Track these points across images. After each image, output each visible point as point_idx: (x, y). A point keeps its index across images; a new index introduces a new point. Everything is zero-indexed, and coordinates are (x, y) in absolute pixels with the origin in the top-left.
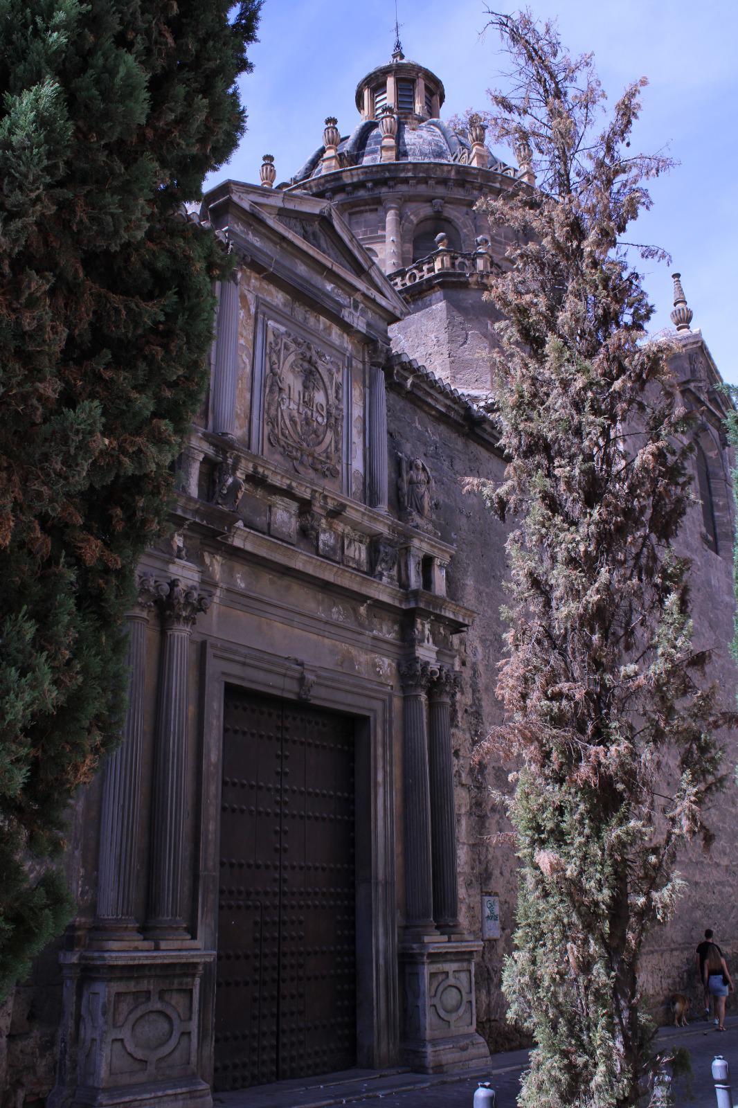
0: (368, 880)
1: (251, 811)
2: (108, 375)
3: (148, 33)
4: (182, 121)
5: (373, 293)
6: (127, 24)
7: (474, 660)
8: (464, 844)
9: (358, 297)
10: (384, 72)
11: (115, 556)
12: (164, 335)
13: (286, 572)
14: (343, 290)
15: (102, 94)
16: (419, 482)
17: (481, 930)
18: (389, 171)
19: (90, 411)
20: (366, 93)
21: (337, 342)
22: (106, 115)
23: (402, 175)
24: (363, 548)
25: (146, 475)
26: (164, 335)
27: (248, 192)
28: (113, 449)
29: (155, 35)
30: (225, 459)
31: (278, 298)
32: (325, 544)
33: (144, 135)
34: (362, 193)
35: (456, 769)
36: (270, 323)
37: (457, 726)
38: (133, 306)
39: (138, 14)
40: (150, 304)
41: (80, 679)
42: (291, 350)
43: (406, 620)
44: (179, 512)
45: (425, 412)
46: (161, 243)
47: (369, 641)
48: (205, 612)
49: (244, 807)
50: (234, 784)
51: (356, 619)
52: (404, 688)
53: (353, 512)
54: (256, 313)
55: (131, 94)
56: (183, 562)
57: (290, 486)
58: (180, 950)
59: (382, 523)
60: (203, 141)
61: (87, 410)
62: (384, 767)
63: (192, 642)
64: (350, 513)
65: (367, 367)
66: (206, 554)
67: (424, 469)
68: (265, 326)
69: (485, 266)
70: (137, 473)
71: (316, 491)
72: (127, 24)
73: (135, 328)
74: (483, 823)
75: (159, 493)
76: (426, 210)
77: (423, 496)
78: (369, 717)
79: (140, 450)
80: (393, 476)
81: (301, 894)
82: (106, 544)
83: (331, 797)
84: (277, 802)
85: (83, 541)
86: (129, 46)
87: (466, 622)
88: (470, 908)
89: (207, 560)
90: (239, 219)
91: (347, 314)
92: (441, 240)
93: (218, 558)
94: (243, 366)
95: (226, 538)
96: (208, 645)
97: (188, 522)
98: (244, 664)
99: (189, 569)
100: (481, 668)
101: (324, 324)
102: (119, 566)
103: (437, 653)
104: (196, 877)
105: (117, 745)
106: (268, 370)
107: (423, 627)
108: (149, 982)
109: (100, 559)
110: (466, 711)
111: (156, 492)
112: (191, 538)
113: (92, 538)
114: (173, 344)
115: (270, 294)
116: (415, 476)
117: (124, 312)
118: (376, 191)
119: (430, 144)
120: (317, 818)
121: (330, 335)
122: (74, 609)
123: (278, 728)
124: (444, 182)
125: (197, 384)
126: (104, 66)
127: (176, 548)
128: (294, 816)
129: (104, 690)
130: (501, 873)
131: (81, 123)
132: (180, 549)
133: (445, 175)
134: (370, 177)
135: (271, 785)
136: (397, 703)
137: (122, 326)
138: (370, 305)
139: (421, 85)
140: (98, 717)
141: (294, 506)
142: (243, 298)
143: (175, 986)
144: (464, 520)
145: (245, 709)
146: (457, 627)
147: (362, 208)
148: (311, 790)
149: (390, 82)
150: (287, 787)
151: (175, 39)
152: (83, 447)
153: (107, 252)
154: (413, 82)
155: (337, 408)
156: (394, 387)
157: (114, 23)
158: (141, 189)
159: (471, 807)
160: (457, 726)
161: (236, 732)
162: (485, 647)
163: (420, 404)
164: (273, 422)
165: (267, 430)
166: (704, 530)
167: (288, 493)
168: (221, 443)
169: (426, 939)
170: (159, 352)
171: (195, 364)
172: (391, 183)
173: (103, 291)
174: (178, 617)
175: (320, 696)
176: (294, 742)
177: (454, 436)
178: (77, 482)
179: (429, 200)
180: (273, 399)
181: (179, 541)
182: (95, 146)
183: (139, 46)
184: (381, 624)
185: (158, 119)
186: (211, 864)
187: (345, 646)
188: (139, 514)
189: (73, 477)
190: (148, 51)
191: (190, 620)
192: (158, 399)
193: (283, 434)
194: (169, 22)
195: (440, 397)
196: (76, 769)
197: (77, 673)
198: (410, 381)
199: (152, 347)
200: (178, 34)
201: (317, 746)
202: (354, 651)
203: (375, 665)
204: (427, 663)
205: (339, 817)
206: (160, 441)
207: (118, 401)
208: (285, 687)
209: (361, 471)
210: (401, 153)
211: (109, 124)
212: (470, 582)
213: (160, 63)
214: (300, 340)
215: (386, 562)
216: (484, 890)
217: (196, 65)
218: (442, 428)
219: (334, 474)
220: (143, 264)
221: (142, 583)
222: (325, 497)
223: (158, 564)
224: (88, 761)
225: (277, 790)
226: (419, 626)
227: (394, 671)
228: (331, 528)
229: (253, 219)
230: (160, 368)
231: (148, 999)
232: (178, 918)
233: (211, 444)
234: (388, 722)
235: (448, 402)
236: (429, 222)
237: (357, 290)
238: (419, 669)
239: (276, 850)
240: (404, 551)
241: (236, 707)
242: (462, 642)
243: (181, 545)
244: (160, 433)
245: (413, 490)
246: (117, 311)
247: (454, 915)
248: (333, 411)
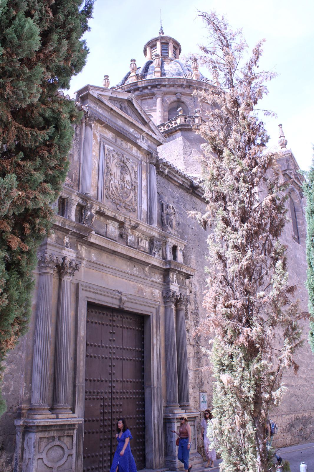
0: (150, 386)
1: (99, 357)
2: (22, 163)
3: (41, 11)
4: (56, 51)
5: (150, 133)
6: (31, 7)
7: (195, 290)
8: (192, 370)
9: (144, 135)
10: (156, 40)
11: (26, 245)
12: (48, 145)
13: (114, 253)
14: (137, 131)
15: (17, 36)
16: (171, 214)
17: (199, 407)
18: (158, 81)
19: (11, 179)
20: (148, 49)
21: (135, 154)
22: (20, 46)
23: (163, 83)
24: (147, 242)
25: (40, 209)
26: (48, 145)
27: (96, 90)
28: (23, 197)
29: (44, 12)
30: (87, 204)
31: (110, 135)
32: (130, 241)
33: (39, 57)
34: (146, 91)
35: (188, 337)
36: (106, 146)
38: (34, 133)
39: (36, 3)
40: (42, 132)
41: (7, 302)
42: (115, 157)
43: (166, 273)
44: (67, 227)
45: (173, 184)
46: (48, 105)
47: (150, 282)
48: (78, 271)
49: (96, 355)
50: (91, 345)
51: (144, 273)
52: (165, 303)
53: (142, 227)
54: (100, 141)
55: (31, 37)
56: (69, 249)
57: (115, 216)
58: (67, 418)
59: (155, 231)
60: (66, 59)
61: (9, 178)
62: (156, 337)
63: (73, 283)
64: (141, 227)
66: (79, 245)
67: (173, 208)
68: (104, 147)
69: (199, 122)
70: (34, 207)
71: (126, 218)
72: (31, 7)
73: (35, 143)
74: (200, 361)
75: (46, 217)
76: (174, 98)
77: (172, 220)
78: (149, 316)
79: (36, 197)
80: (160, 211)
81: (121, 393)
82: (23, 240)
83: (134, 350)
84: (110, 353)
85: (11, 238)
86: (32, 17)
87: (192, 274)
88: (195, 398)
89: (79, 248)
90: (92, 101)
91: (139, 142)
92: (180, 111)
93: (84, 247)
94: (94, 164)
95: (87, 238)
96: (80, 285)
97: (70, 232)
98: (95, 293)
99: (71, 252)
100: (198, 294)
101: (130, 146)
102: (28, 250)
103: (179, 287)
104: (75, 386)
105: (27, 331)
106: (105, 166)
107: (173, 276)
109: (19, 247)
110: (192, 312)
111: (45, 217)
112: (72, 238)
113: (15, 237)
114: (53, 150)
115: (107, 134)
116: (169, 211)
117: (30, 136)
118: (153, 90)
119: (175, 70)
120: (127, 360)
121: (132, 151)
122: (5, 269)
123: (110, 320)
124: (181, 86)
125: (64, 168)
126: (19, 24)
127: (65, 243)
128: (117, 359)
129: (20, 306)
130: (208, 383)
131: (8, 50)
132: (67, 244)
133: (182, 83)
134: (150, 84)
135: (107, 346)
136: (162, 309)
137: (29, 142)
138: (149, 138)
139: (171, 45)
140: (17, 318)
141: (117, 224)
142: (95, 135)
143: (66, 434)
144: (190, 230)
145: (96, 313)
146: (188, 276)
147: (146, 97)
148: (125, 347)
149: (158, 44)
150: (114, 346)
151: (54, 15)
152: (7, 195)
153: (21, 109)
154: (168, 44)
155: (135, 182)
156: (160, 173)
157: (25, 6)
158: (36, 80)
159: (194, 354)
160: (188, 319)
161: (92, 322)
162: (200, 285)
163: (171, 180)
164: (108, 188)
165: (105, 192)
166: (293, 233)
167: (114, 219)
168: (85, 197)
169: (176, 412)
170: (46, 154)
171: (63, 159)
172: (159, 87)
173: (20, 126)
174: (67, 273)
175: (128, 307)
176: (118, 326)
177: (186, 194)
178: (5, 211)
179: (175, 94)
180: (107, 179)
181: (67, 240)
182: (15, 60)
183: (37, 17)
184: (155, 275)
185: (45, 49)
186: (81, 380)
187: (139, 285)
188: (37, 226)
189: (3, 208)
190: (41, 19)
191: (72, 274)
192: (46, 175)
193: (112, 194)
194: (51, 7)
195: (180, 177)
196: (7, 342)
197: (6, 299)
198: (166, 171)
199: (43, 151)
200: (55, 13)
201: (127, 328)
202: (143, 287)
203: (152, 293)
204: (175, 292)
205: (137, 359)
206: (45, 193)
207: (26, 175)
208: (114, 303)
209: (146, 209)
210: (163, 74)
211: (21, 50)
212: (193, 256)
213: (46, 25)
214: (119, 153)
215: (157, 248)
216: (201, 390)
217: (63, 26)
218: (181, 190)
219: (134, 210)
220: (39, 114)
221: (51, 258)
222: (130, 220)
223: (58, 250)
224: (12, 339)
225: (110, 348)
226: (171, 276)
227: (161, 295)
228: (133, 234)
229: (99, 101)
230: (47, 161)
231: (54, 440)
232: (67, 404)
233: (81, 198)
234: (158, 318)
235: (183, 180)
236: (175, 103)
237: (144, 131)
238: (171, 294)
239: (110, 374)
240: (165, 243)
241: (92, 312)
242: (190, 283)
243: (68, 241)
244: (45, 189)
245: (168, 217)
246: (27, 135)
247: (188, 401)
248: (134, 184)
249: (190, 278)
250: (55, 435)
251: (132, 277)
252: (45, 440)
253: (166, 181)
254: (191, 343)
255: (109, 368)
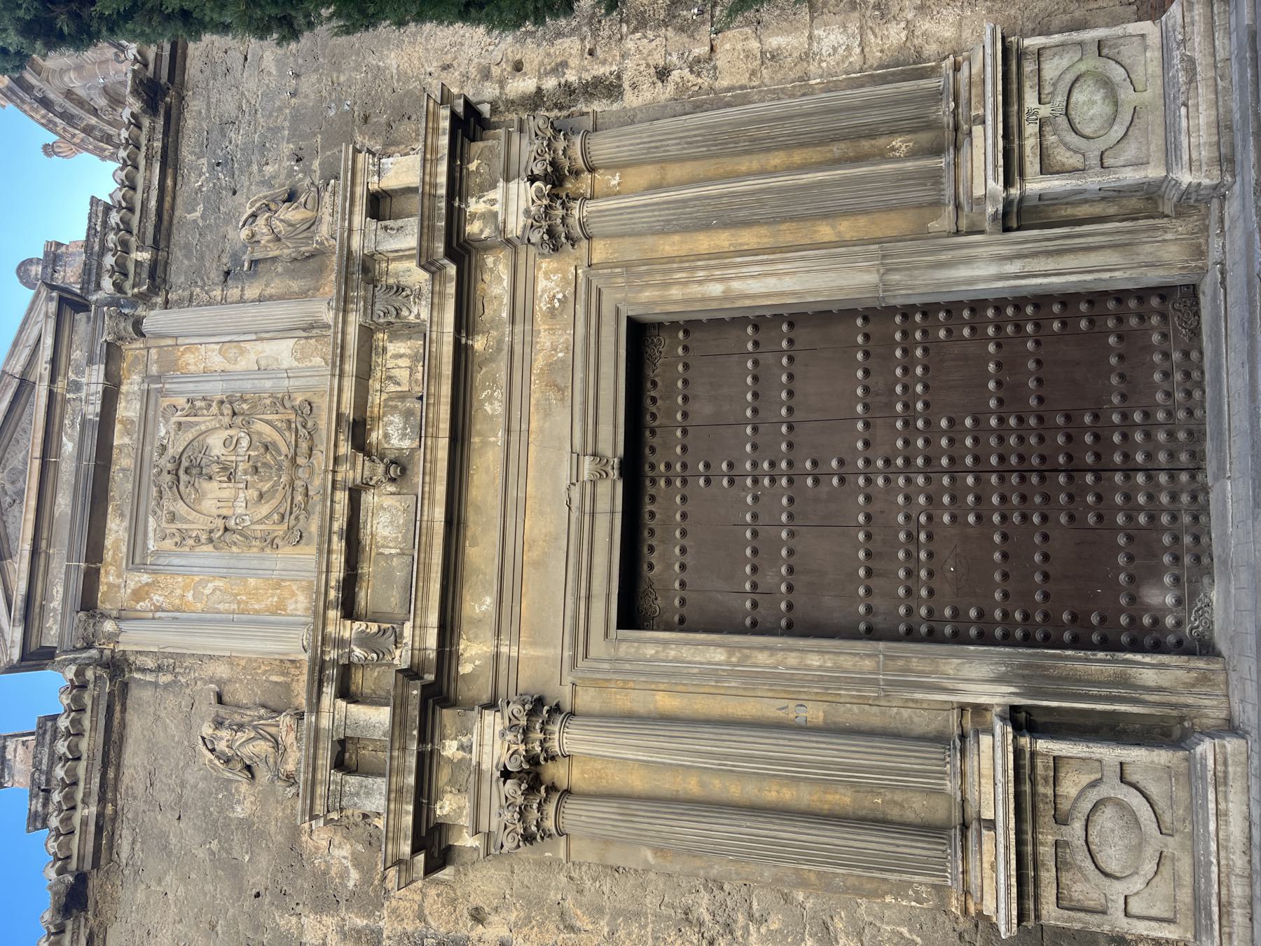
37: (619, 77)
45: (174, 198)
58: (995, 784)
62: (700, 282)
65: (151, 342)
90: (41, 629)
99: (481, 735)
108: (1042, 844)
115: (117, 548)
116: (267, 238)
132: (461, 747)
143: (1050, 792)
163: (166, 217)
203: (552, 312)
208: (610, 495)
209: (291, 342)
231: (1067, 844)
235: (142, 163)
237: (51, 395)
249: (467, 103)
250: (1051, 839)
251: (515, 425)
252: (1066, 878)
253: (178, 237)
254: (707, 48)
255: (823, 489)
